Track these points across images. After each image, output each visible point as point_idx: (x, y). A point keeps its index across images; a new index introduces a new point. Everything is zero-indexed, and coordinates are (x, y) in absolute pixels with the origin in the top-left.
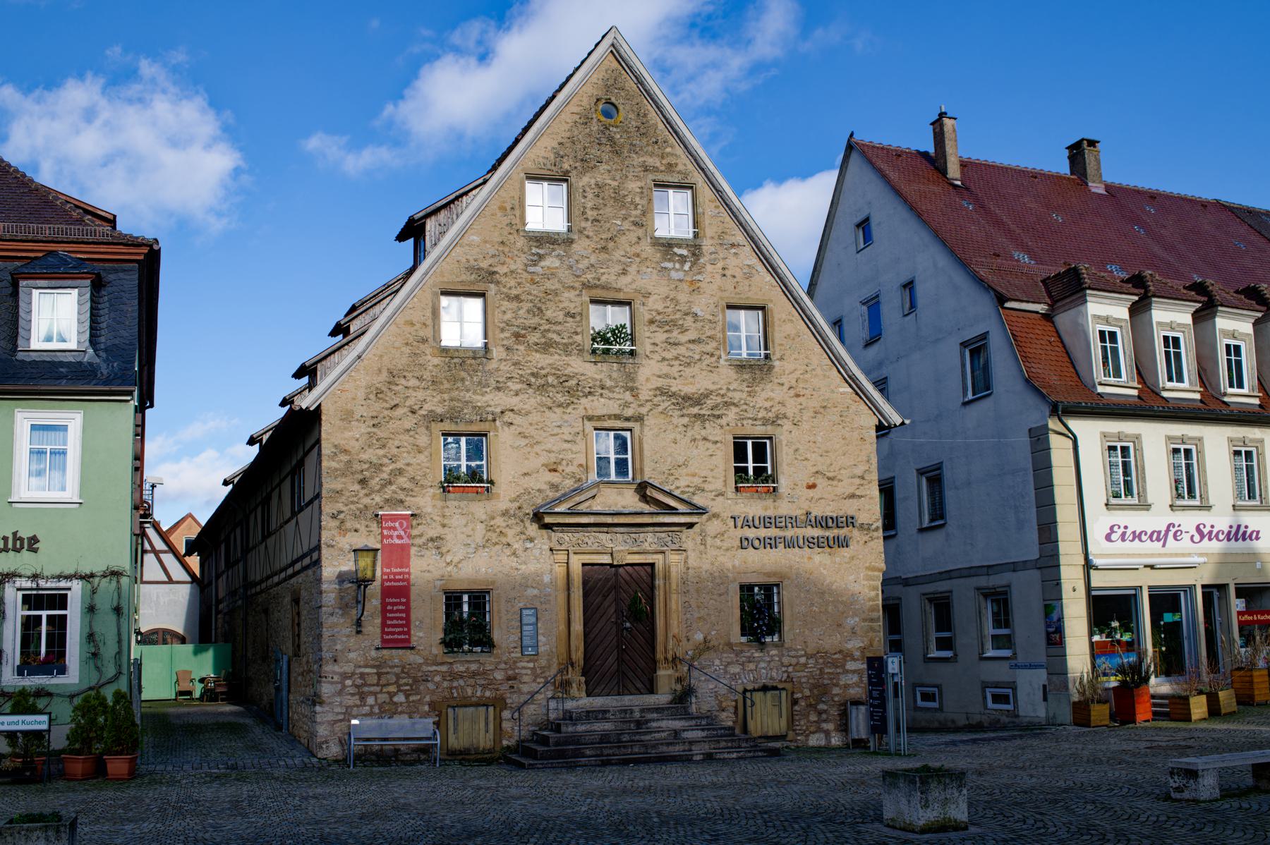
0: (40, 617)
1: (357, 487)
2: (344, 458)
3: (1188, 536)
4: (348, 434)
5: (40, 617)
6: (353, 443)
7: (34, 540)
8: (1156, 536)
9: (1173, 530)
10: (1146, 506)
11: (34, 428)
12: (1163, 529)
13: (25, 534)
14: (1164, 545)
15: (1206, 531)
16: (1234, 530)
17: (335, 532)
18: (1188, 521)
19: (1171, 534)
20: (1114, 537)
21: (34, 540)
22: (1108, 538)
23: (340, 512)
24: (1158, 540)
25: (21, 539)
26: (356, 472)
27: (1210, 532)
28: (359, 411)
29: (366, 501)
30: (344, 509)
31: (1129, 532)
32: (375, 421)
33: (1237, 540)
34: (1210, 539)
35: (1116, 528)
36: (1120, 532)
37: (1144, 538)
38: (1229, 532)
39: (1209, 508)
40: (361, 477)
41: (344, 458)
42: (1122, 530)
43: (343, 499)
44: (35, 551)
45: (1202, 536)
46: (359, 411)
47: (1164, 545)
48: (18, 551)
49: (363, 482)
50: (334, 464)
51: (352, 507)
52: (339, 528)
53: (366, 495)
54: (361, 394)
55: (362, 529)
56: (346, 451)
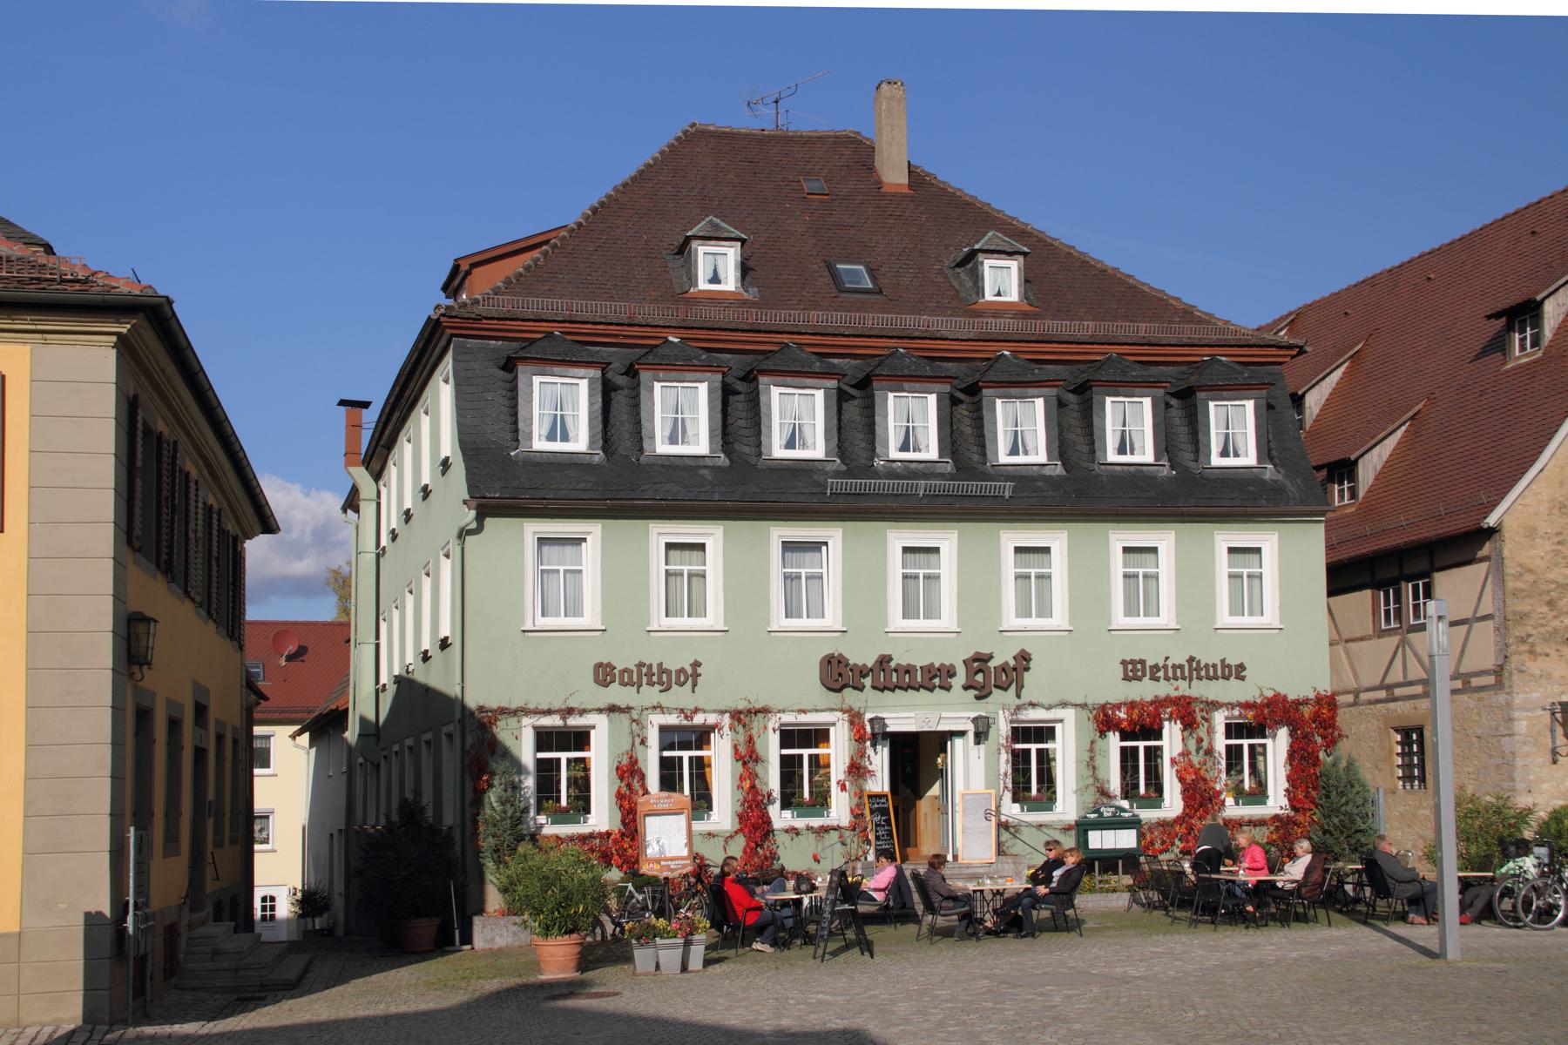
0: (1241, 746)
1: (1545, 609)
2: (1530, 578)
4: (1533, 552)
5: (1241, 746)
6: (1539, 562)
7: (1241, 667)
11: (1232, 550)
13: (1233, 661)
17: (1525, 657)
21: (1241, 667)
23: (1529, 636)
25: (1229, 666)
26: (1543, 593)
28: (1544, 528)
29: (1556, 623)
30: (1533, 632)
32: (1560, 538)
40: (1547, 598)
41: (1530, 578)
43: (1531, 622)
44: (1243, 678)
46: (1544, 528)
48: (1227, 678)
49: (1550, 603)
50: (1520, 585)
51: (1542, 630)
52: (1531, 652)
53: (1556, 617)
54: (1543, 509)
55: (1553, 654)
56: (1530, 570)
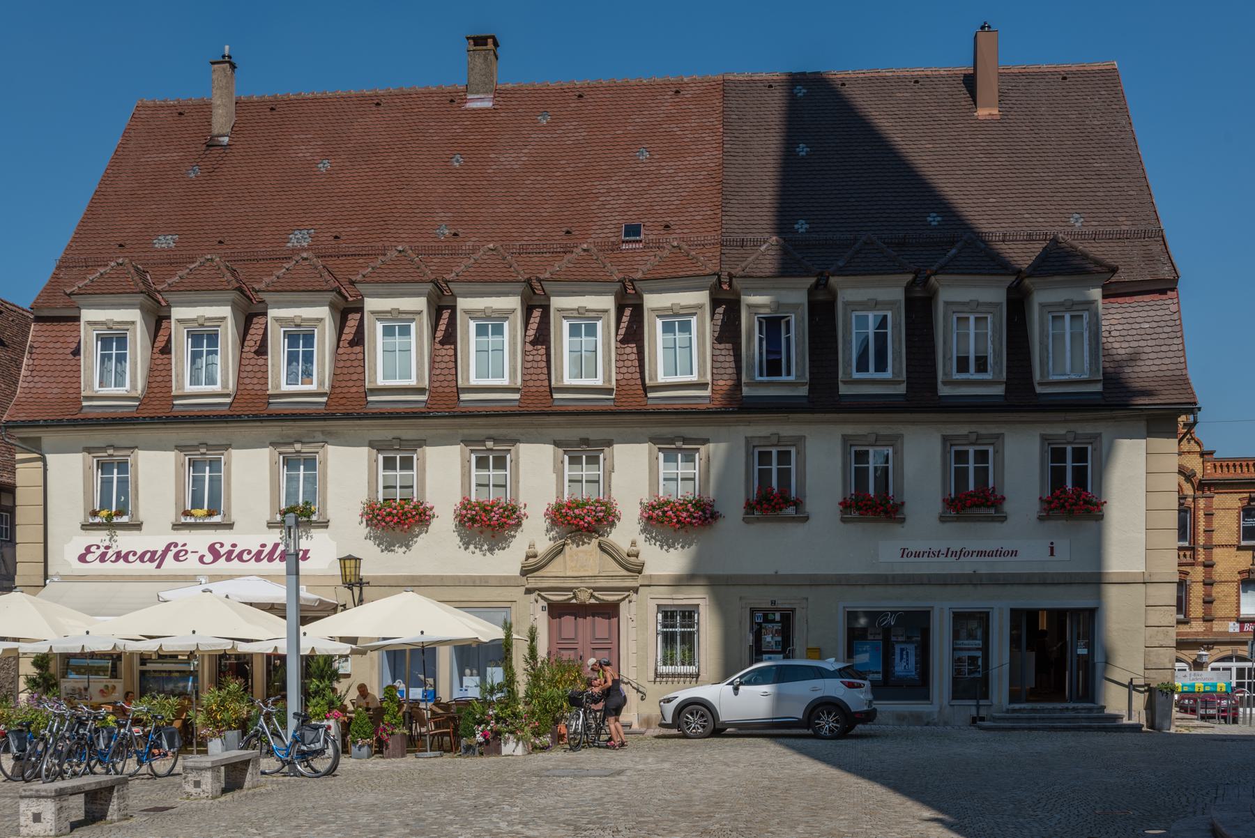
3: (197, 556)
8: (155, 557)
9: (174, 550)
10: (137, 526)
12: (160, 549)
14: (159, 566)
15: (223, 551)
16: (267, 550)
18: (198, 541)
19: (171, 555)
20: (89, 557)
22: (82, 559)
24: (152, 560)
27: (230, 553)
31: (111, 552)
33: (271, 559)
34: (229, 559)
35: (93, 549)
36: (99, 552)
37: (131, 558)
38: (259, 553)
39: (230, 526)
42: (102, 549)
45: (216, 556)
47: (159, 566)
